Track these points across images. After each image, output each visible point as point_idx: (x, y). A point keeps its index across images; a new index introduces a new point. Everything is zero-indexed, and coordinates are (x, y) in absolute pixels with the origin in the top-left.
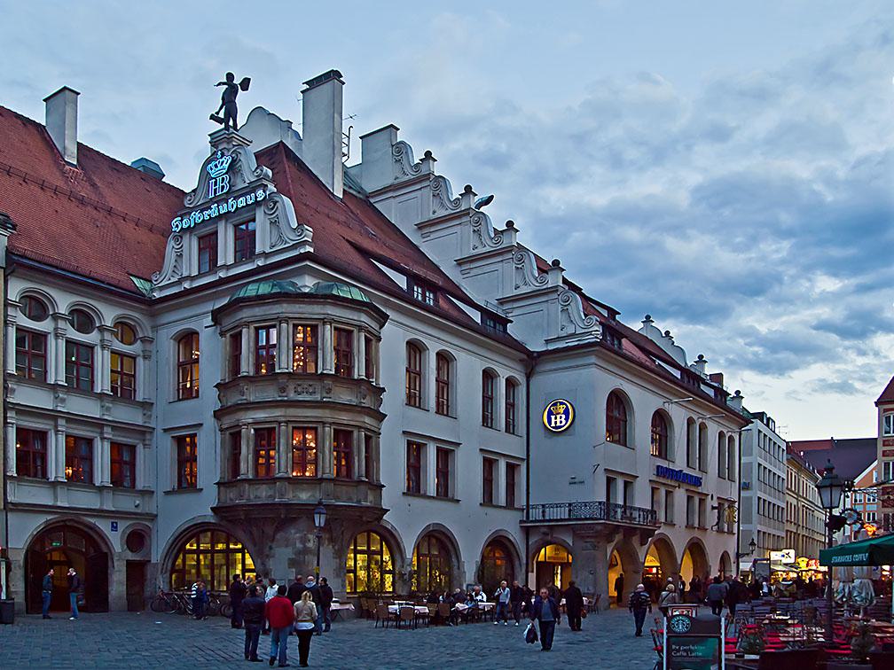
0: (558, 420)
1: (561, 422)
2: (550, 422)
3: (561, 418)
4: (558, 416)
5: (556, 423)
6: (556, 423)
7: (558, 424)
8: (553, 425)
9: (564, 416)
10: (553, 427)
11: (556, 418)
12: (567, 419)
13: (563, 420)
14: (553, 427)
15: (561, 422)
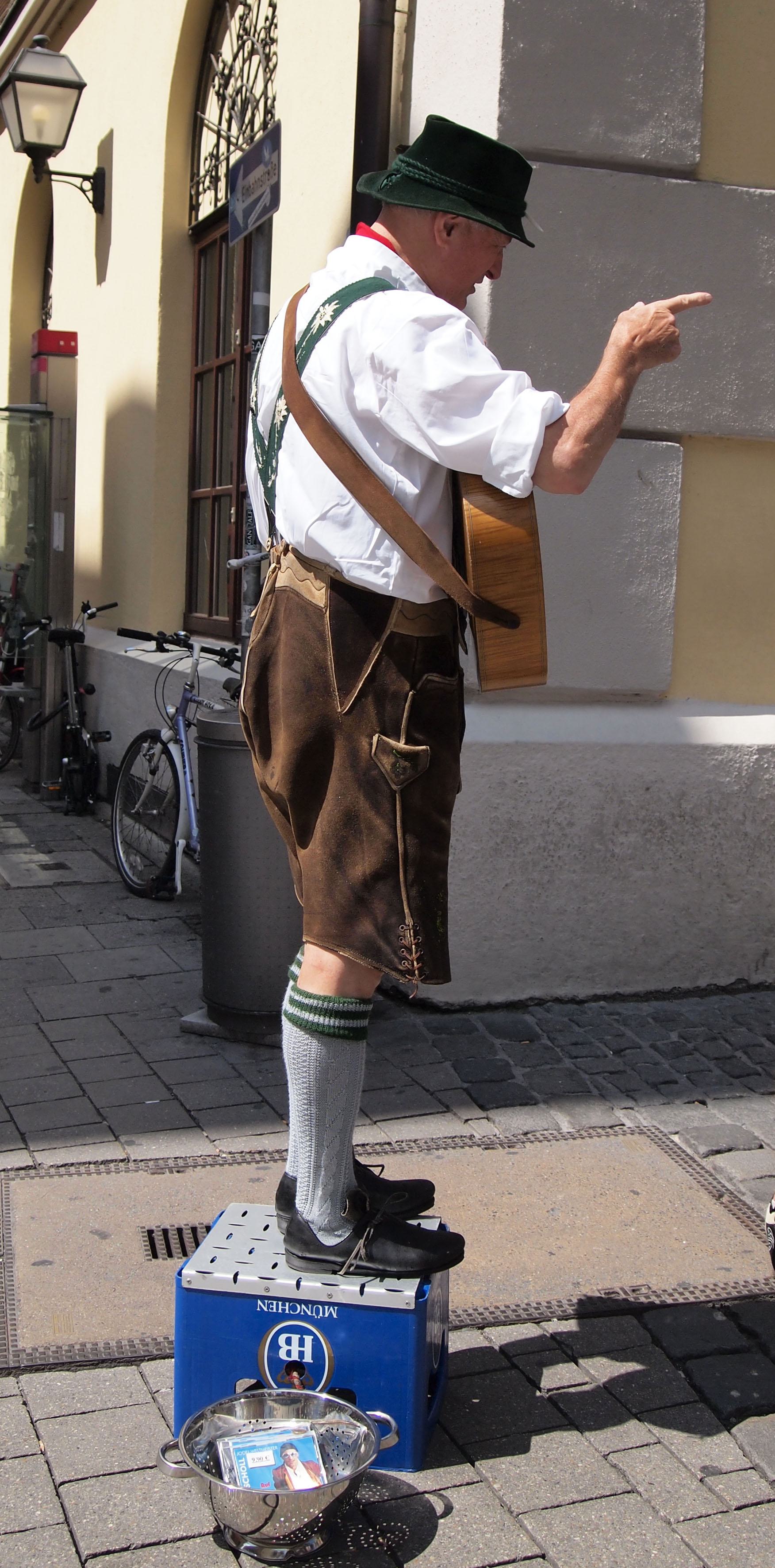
0: (295, 1349)
1: (288, 1342)
2: (316, 1342)
3: (289, 1353)
4: (295, 1357)
5: (302, 1343)
6: (302, 1343)
7: (295, 1338)
8: (308, 1339)
9: (282, 1355)
10: (310, 1333)
11: (301, 1354)
12: (275, 1346)
13: (284, 1348)
14: (310, 1333)
15: (288, 1342)
